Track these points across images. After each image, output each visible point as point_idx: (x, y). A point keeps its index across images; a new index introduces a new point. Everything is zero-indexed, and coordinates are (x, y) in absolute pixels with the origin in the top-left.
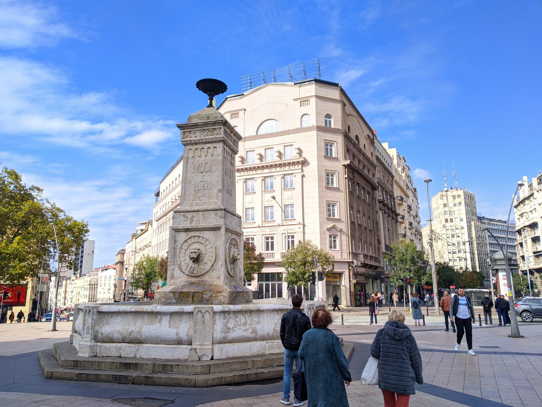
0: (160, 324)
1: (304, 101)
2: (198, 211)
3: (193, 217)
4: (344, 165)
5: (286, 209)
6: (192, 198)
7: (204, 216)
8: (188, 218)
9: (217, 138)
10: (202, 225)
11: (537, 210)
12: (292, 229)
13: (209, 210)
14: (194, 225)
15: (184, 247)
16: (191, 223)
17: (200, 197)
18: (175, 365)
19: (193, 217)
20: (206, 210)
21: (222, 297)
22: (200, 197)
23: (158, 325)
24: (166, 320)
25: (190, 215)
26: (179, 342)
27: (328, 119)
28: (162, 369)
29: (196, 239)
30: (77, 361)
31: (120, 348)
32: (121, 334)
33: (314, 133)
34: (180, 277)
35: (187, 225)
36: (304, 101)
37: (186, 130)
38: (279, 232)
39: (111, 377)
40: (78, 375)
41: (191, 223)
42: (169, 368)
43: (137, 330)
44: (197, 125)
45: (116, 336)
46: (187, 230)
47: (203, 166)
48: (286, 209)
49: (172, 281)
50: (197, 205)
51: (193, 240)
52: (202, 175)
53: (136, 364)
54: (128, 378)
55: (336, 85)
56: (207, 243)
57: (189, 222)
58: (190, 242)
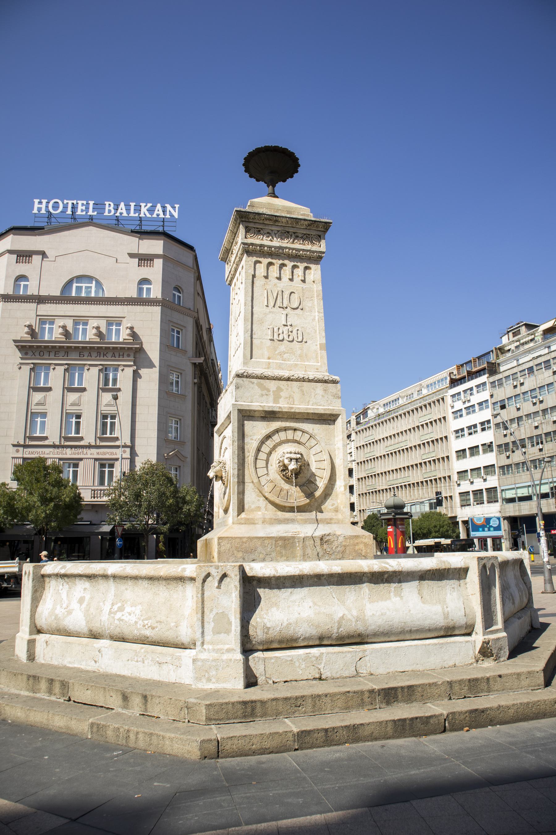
0: (401, 597)
1: (145, 259)
2: (288, 379)
3: (279, 389)
4: (195, 364)
5: (106, 421)
6: (266, 354)
7: (302, 391)
8: (268, 390)
9: (314, 252)
10: (300, 407)
11: (353, 454)
12: (112, 454)
13: (310, 381)
14: (283, 405)
15: (265, 449)
16: (276, 400)
17: (285, 353)
18: (494, 677)
19: (279, 389)
20: (303, 380)
21: (361, 546)
22: (285, 353)
23: (396, 600)
24: (410, 589)
25: (272, 385)
26: (448, 632)
27: (177, 294)
28: (469, 689)
29: (290, 434)
30: (252, 702)
31: (318, 658)
32: (318, 626)
33: (157, 310)
34: (259, 508)
35: (269, 404)
36: (145, 259)
37: (251, 225)
38: (89, 456)
39: (390, 725)
40: (303, 734)
41: (276, 400)
42: (484, 686)
43: (355, 613)
44: (276, 221)
45: (304, 630)
46: (269, 416)
47: (286, 295)
48: (106, 421)
49: (243, 515)
50: (280, 367)
51: (282, 436)
52: (285, 312)
53: (410, 687)
54: (432, 721)
55: (191, 248)
56: (313, 442)
57: (271, 398)
58: (276, 438)
